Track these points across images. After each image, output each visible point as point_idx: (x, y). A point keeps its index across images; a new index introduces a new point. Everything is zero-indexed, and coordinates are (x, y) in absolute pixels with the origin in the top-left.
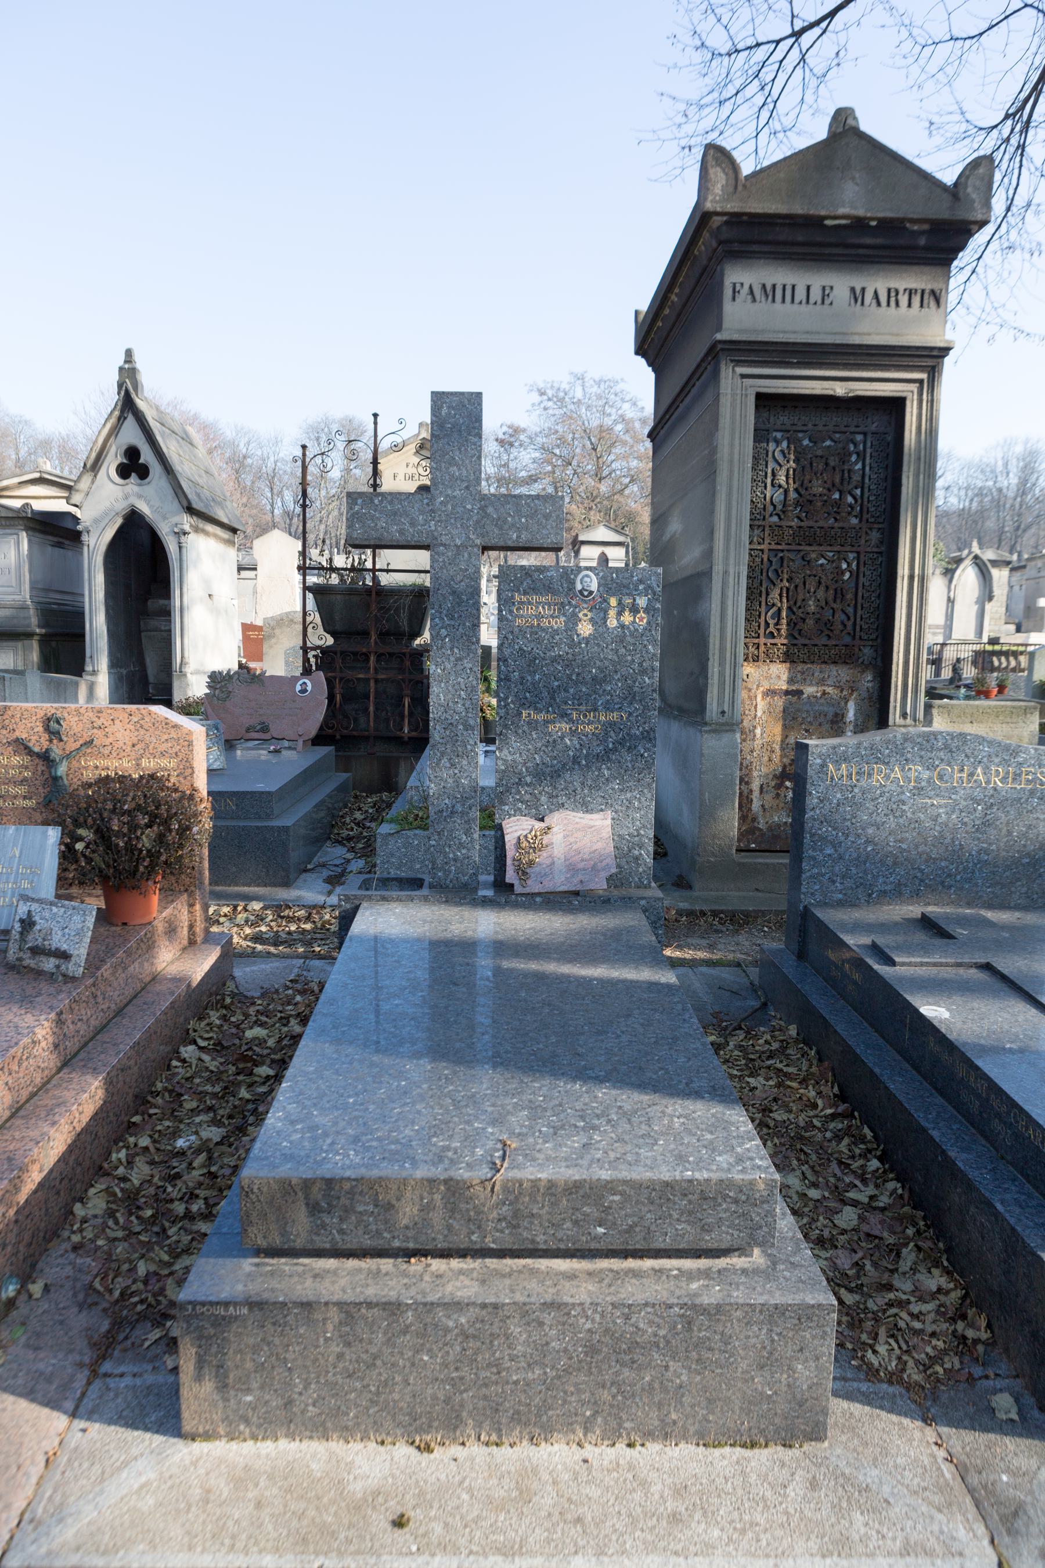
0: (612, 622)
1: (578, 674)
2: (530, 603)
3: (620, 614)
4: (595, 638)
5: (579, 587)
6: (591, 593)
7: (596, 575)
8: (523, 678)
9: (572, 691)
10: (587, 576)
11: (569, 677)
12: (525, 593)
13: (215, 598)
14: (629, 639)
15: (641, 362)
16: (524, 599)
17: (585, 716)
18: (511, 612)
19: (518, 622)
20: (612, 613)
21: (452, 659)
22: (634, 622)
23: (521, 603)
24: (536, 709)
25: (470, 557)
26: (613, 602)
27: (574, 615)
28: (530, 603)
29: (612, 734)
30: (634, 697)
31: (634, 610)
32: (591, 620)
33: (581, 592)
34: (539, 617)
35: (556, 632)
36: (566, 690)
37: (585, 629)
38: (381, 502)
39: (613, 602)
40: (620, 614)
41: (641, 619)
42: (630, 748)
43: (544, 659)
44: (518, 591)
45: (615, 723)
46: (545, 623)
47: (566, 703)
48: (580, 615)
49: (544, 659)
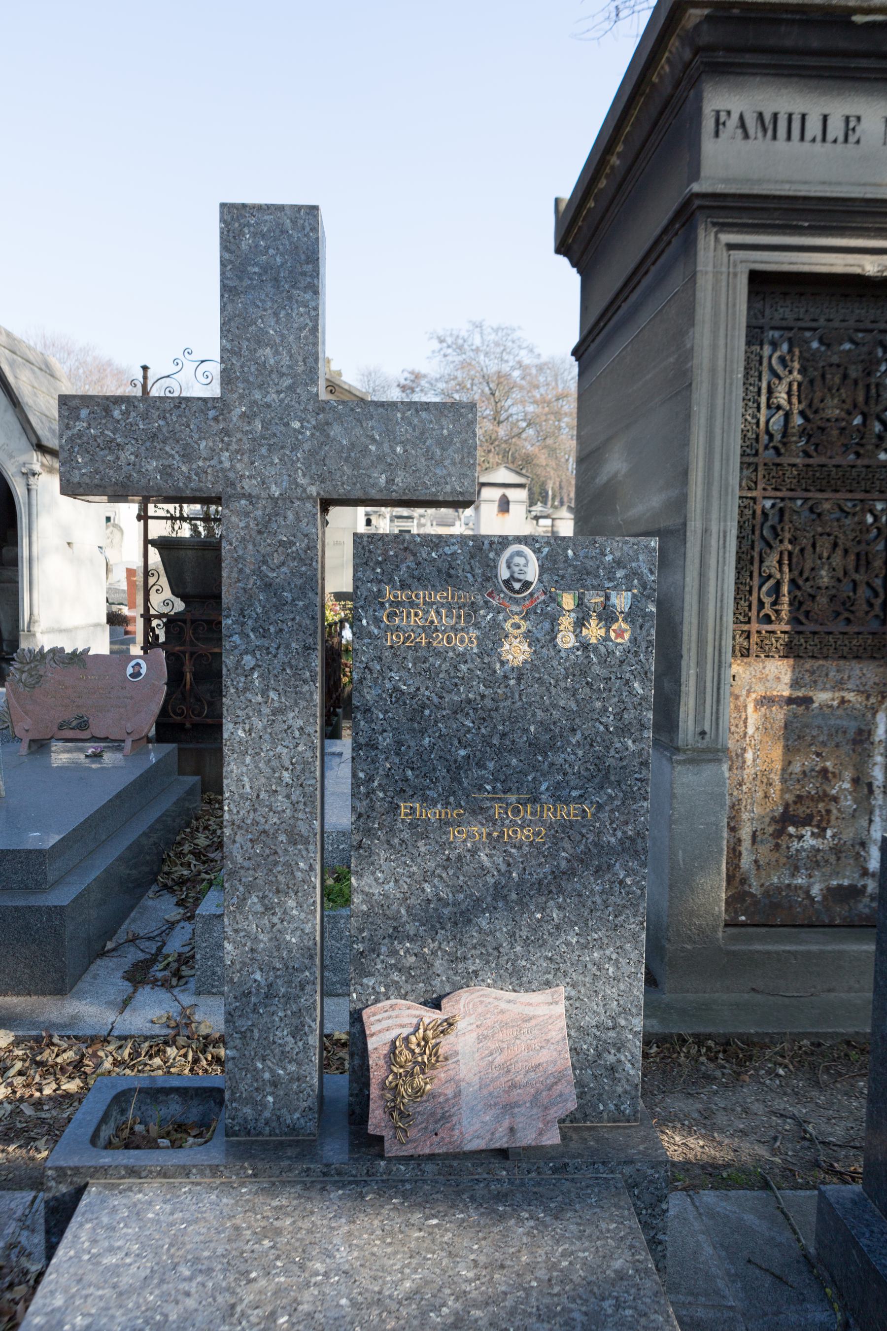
0: (567, 640)
1: (503, 735)
2: (412, 604)
3: (580, 623)
4: (534, 668)
5: (504, 574)
6: (527, 585)
7: (537, 551)
8: (400, 743)
9: (491, 765)
10: (519, 554)
11: (486, 741)
12: (404, 586)
13: (75, 546)
14: (596, 669)
15: (564, 261)
16: (402, 596)
17: (516, 812)
18: (377, 621)
19: (392, 639)
20: (566, 622)
21: (266, 710)
22: (607, 638)
23: (397, 604)
24: (425, 799)
25: (298, 519)
26: (568, 601)
27: (495, 625)
28: (412, 604)
29: (567, 844)
30: (606, 776)
31: (607, 616)
32: (528, 635)
33: (507, 582)
34: (430, 629)
35: (463, 657)
36: (481, 765)
37: (516, 652)
38: (126, 413)
39: (568, 601)
40: (580, 623)
41: (620, 634)
42: (598, 869)
43: (439, 707)
44: (391, 581)
45: (572, 824)
46: (440, 642)
47: (481, 788)
48: (507, 626)
49: (439, 707)
